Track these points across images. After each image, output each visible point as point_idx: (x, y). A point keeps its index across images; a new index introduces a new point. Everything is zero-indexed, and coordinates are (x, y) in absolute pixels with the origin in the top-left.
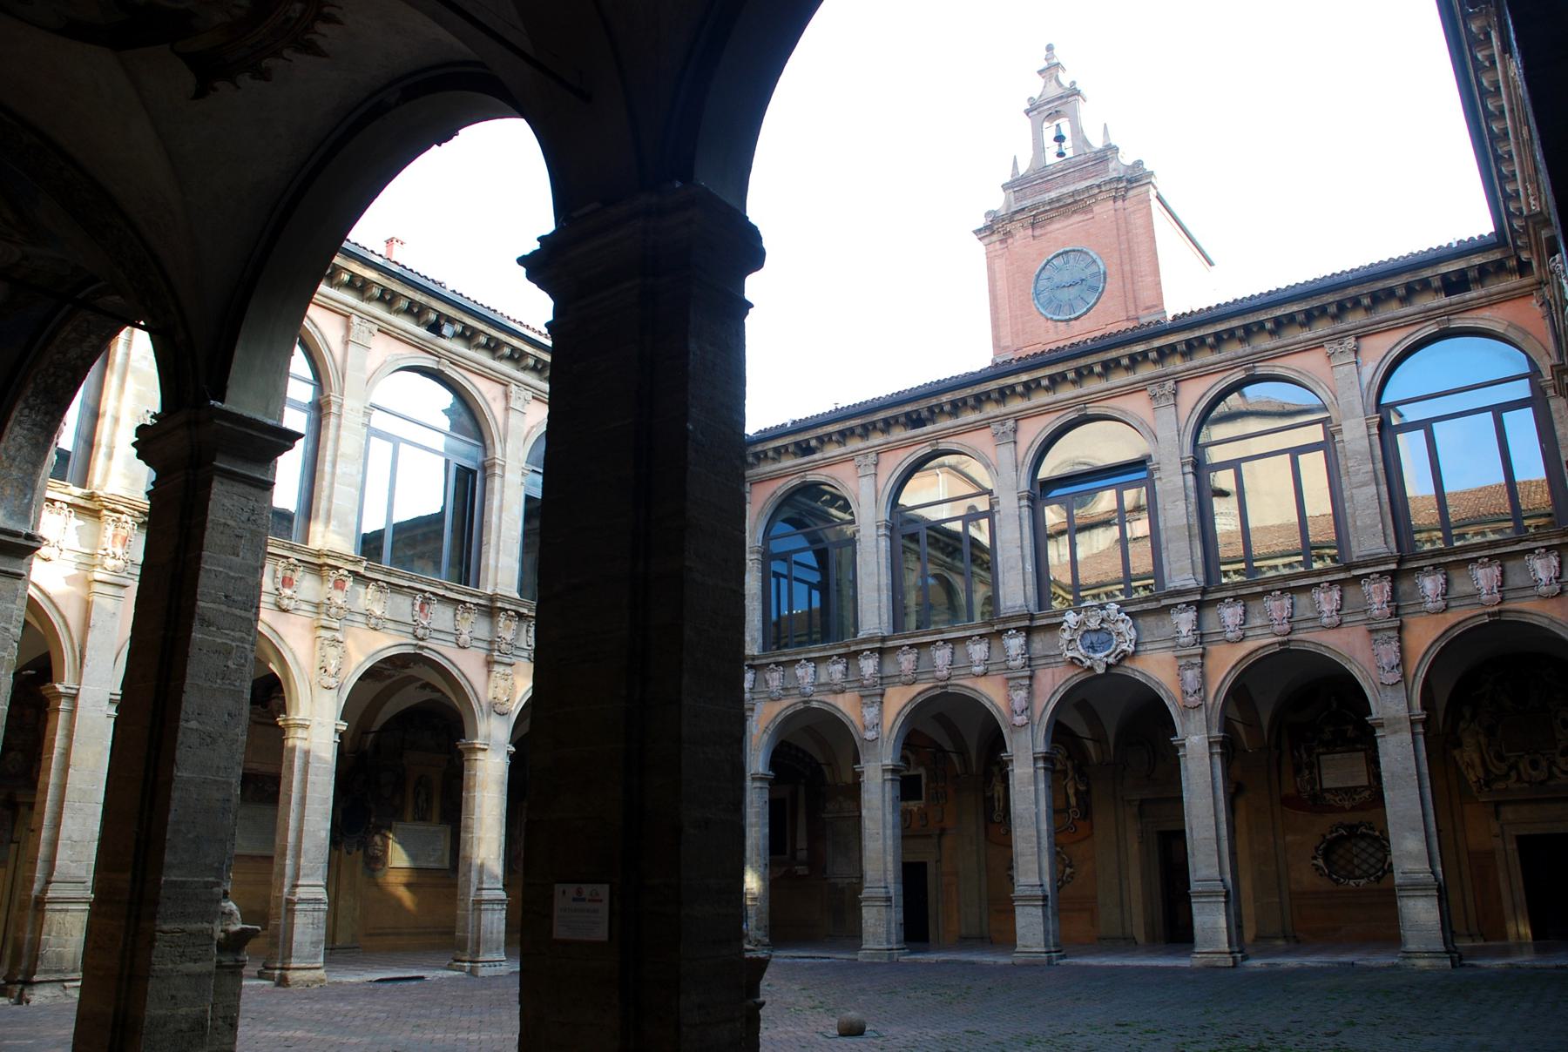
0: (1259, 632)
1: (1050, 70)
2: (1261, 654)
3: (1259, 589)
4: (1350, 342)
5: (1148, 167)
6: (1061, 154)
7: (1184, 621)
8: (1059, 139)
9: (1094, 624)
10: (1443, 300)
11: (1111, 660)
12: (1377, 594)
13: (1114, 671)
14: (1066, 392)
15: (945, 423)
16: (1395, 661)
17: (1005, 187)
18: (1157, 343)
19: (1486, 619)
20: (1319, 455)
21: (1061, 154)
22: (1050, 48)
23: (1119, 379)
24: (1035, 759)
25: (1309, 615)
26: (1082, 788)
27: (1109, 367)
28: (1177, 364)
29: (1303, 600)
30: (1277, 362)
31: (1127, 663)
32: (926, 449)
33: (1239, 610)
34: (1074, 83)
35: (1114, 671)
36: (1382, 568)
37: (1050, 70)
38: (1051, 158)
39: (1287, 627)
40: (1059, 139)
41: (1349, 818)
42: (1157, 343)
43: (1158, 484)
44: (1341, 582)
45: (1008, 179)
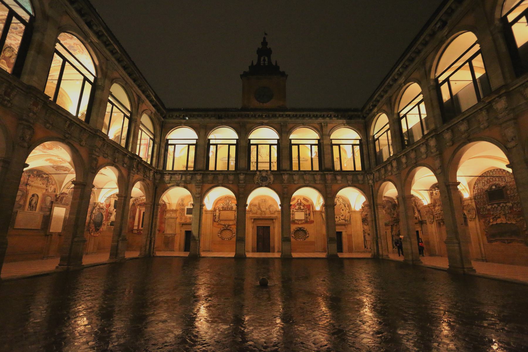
1: (264, 43)
6: (264, 64)
7: (285, 177)
8: (264, 60)
17: (249, 67)
20: (317, 147)
21: (264, 64)
22: (264, 38)
37: (264, 43)
40: (264, 60)
41: (300, 226)
44: (321, 174)
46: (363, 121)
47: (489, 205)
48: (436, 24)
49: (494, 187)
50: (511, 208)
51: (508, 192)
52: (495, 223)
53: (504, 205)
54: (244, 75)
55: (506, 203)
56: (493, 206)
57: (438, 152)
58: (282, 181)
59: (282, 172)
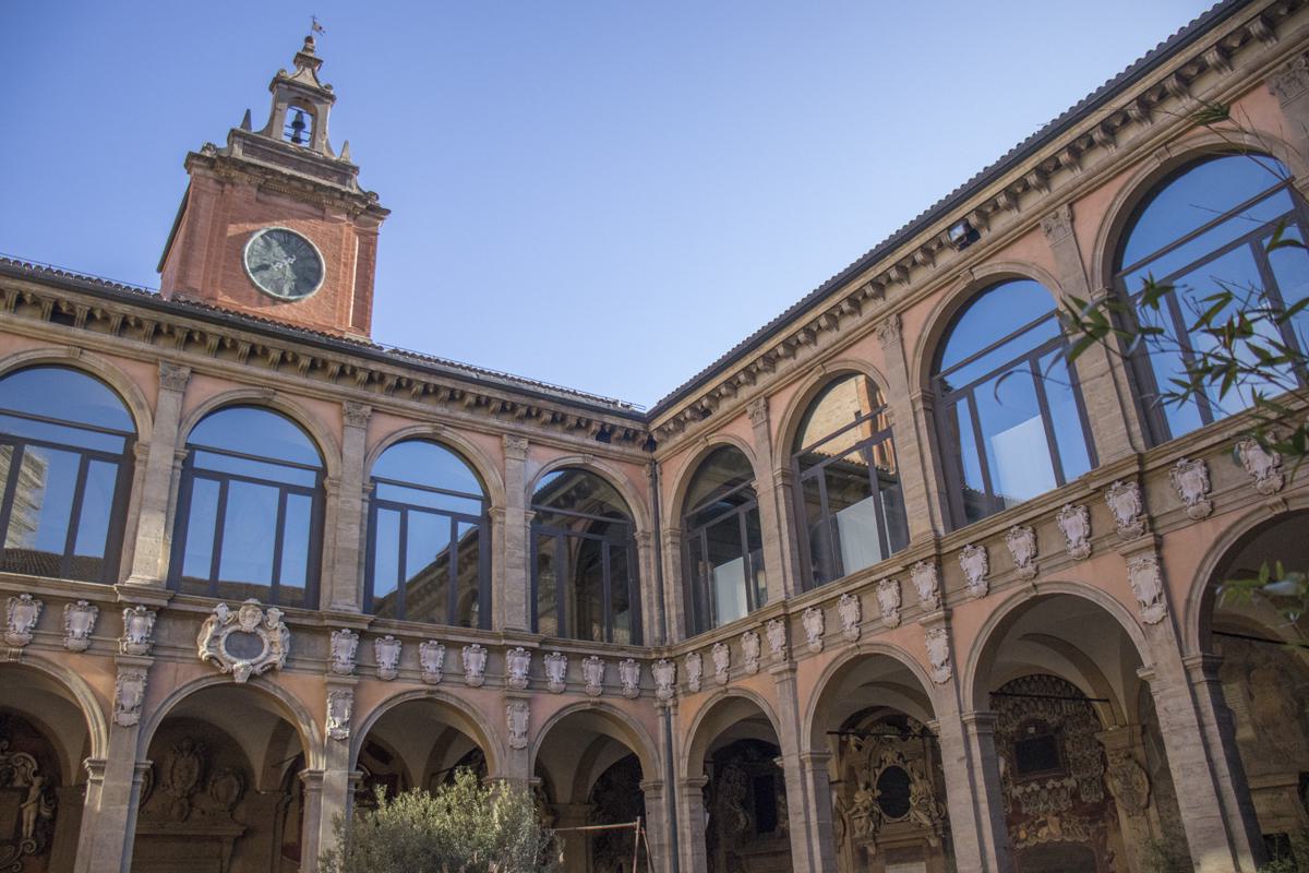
0: (410, 675)
2: (408, 697)
3: (421, 634)
4: (524, 443)
5: (382, 203)
6: (296, 140)
7: (343, 648)
8: (298, 125)
9: (248, 624)
10: (592, 442)
11: (258, 669)
12: (517, 666)
13: (255, 684)
14: (259, 370)
15: (107, 339)
16: (524, 730)
18: (373, 366)
19: (589, 707)
21: (296, 140)
22: (309, 39)
23: (318, 383)
24: (136, 771)
25: (454, 669)
26: (46, 813)
27: (315, 367)
28: (377, 395)
29: (453, 655)
30: (462, 433)
31: (270, 678)
32: (58, 352)
33: (396, 649)
34: (329, 87)
35: (255, 684)
36: (529, 644)
37: (305, 59)
38: (288, 139)
39: (438, 677)
40: (298, 125)
42: (373, 366)
43: (331, 502)
45: (238, 126)
46: (646, 454)
47: (1016, 785)
48: (950, 228)
49: (1032, 730)
50: (1075, 795)
51: (1068, 745)
52: (1032, 842)
53: (1058, 785)
54: (204, 162)
55: (1059, 779)
56: (1029, 790)
57: (941, 613)
58: (325, 663)
59: (327, 622)
